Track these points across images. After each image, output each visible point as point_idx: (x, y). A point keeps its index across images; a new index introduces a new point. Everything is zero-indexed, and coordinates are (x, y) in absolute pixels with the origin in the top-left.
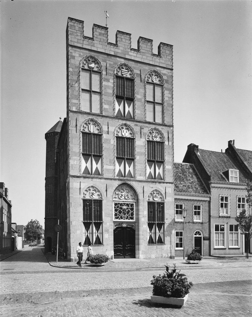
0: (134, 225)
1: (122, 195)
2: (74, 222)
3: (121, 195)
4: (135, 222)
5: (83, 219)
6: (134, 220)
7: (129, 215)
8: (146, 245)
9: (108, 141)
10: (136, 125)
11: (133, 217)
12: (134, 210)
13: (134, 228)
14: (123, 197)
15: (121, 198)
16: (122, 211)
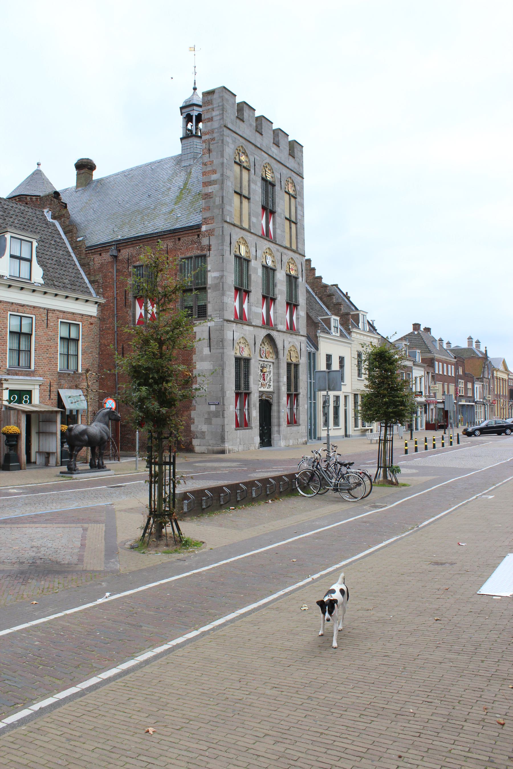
0: (271, 396)
1: (263, 352)
2: (228, 392)
3: (262, 352)
4: (274, 392)
5: (234, 388)
6: (271, 389)
7: (268, 382)
8: (286, 426)
9: (256, 269)
10: (278, 250)
11: (270, 384)
12: (272, 374)
13: (271, 401)
14: (264, 355)
15: (263, 357)
16: (262, 375)
